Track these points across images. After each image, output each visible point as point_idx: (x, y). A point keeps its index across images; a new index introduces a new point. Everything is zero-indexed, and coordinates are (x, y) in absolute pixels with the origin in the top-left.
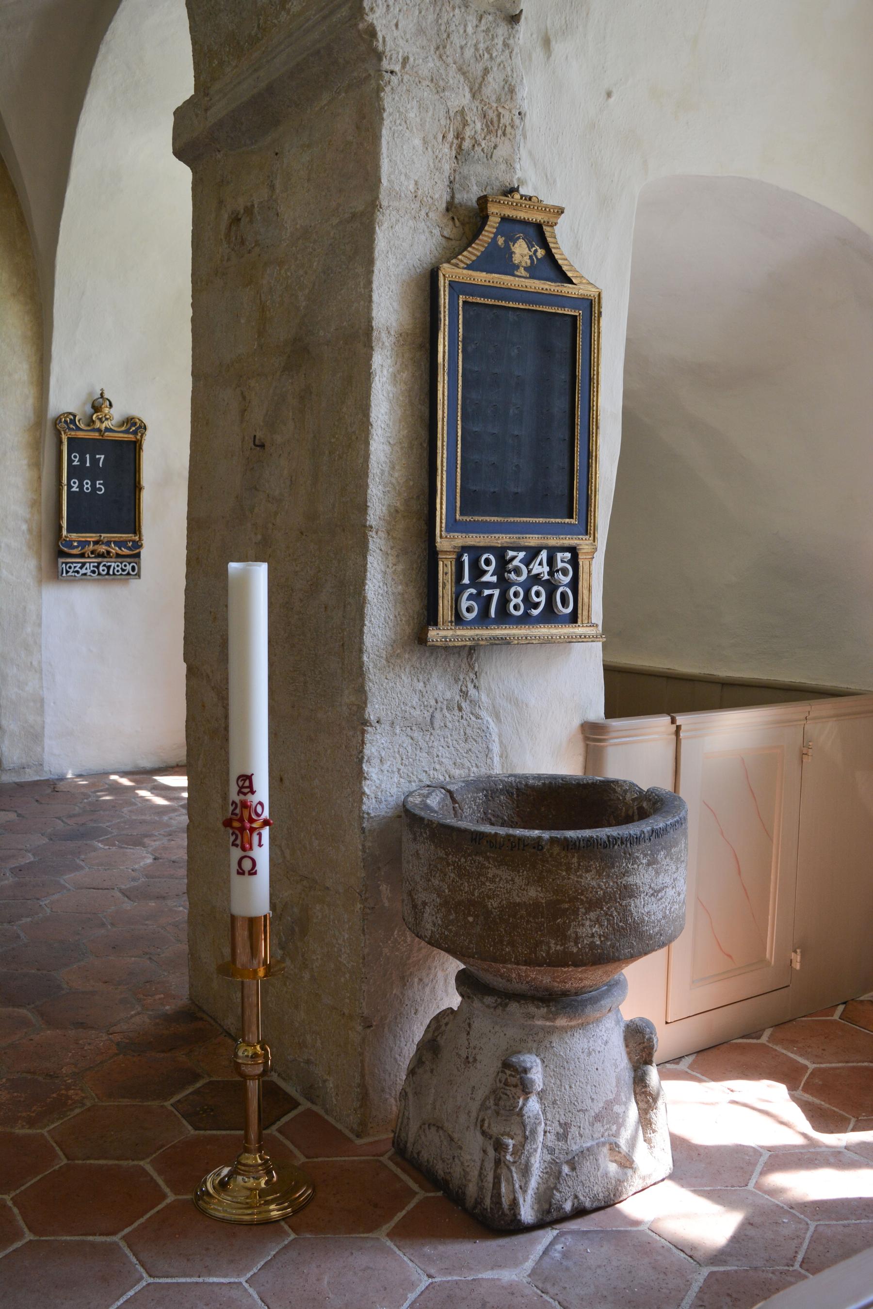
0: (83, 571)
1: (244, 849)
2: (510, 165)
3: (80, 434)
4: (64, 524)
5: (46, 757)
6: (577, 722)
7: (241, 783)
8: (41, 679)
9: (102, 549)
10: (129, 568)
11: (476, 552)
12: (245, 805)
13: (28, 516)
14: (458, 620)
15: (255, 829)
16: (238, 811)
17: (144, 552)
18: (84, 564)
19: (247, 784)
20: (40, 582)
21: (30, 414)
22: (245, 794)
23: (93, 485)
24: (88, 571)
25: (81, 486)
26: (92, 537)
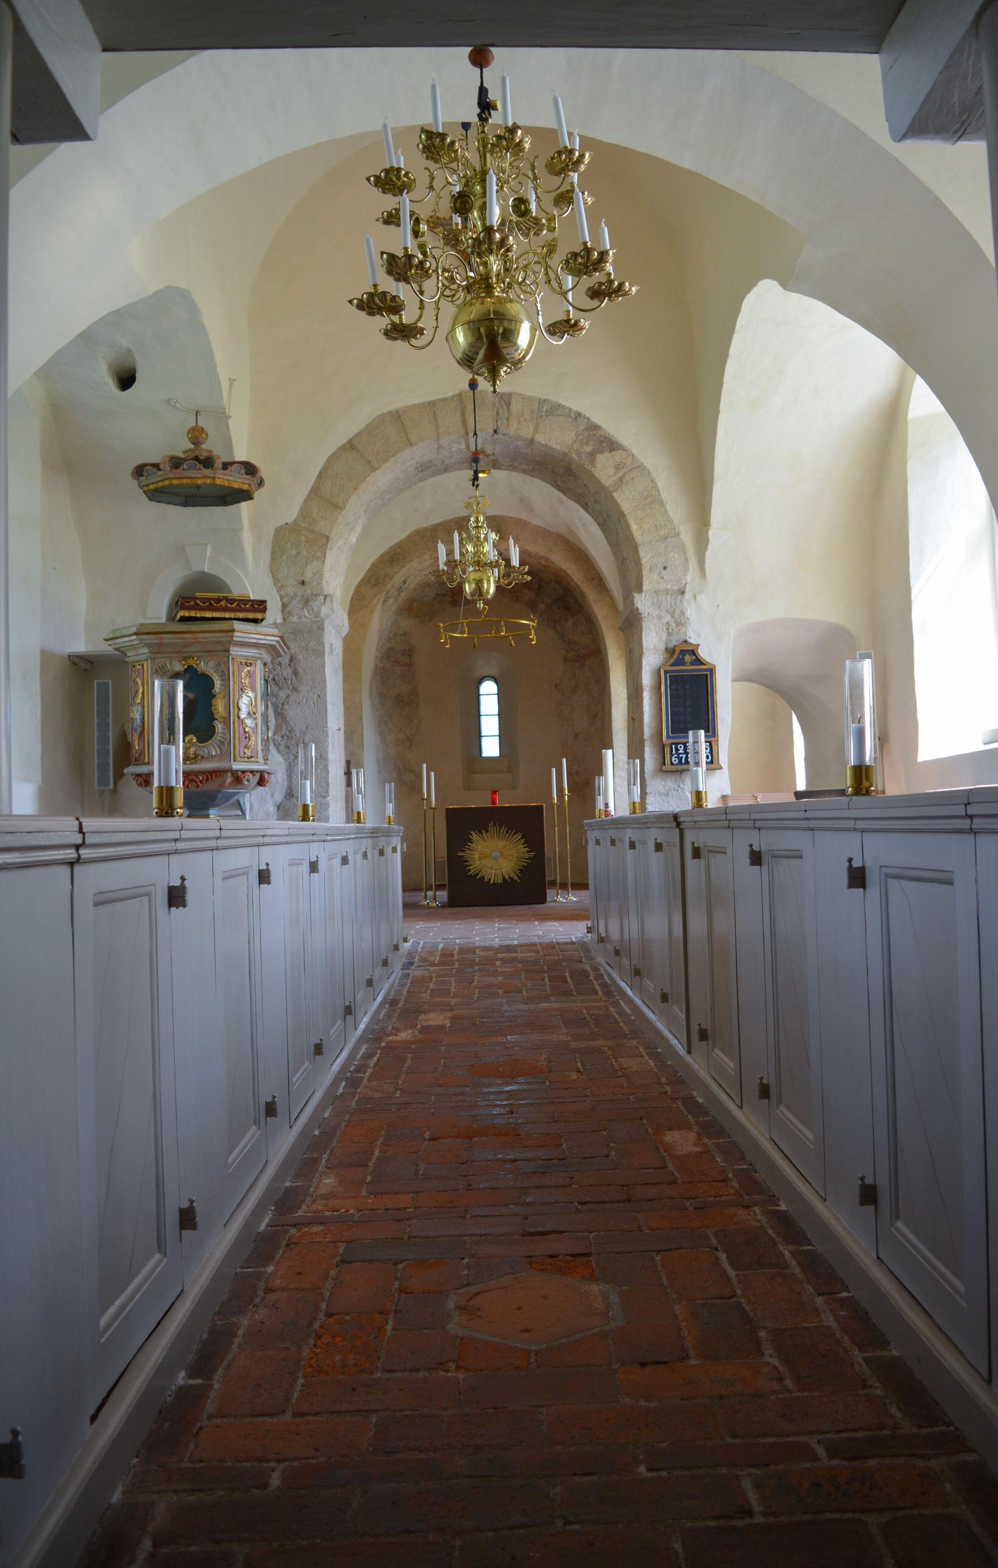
2: (685, 634)
6: (719, 795)
11: (677, 744)
14: (672, 764)
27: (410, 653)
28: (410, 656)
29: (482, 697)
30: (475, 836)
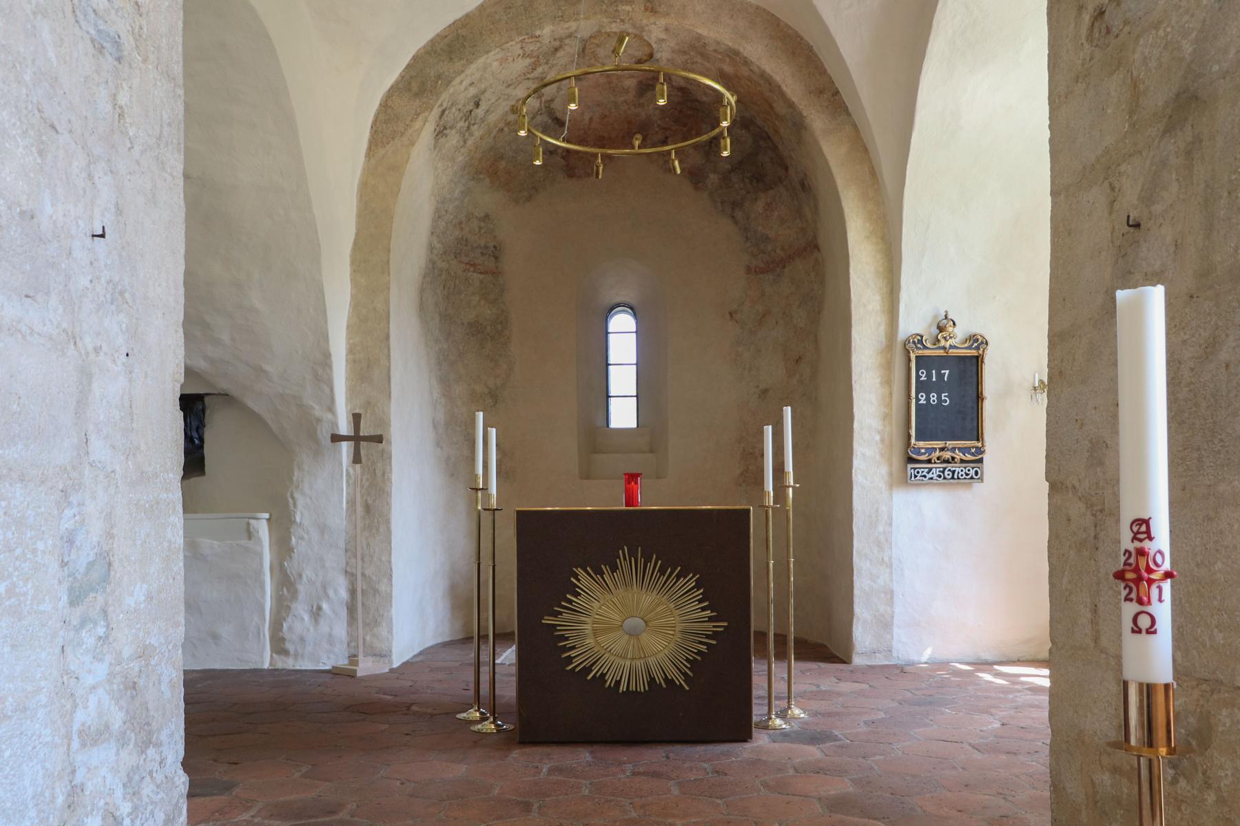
0: (930, 475)
1: (1140, 602)
3: (927, 353)
4: (913, 433)
5: (895, 645)
7: (1135, 529)
8: (891, 573)
9: (947, 455)
10: (972, 472)
12: (1141, 553)
13: (881, 428)
15: (1154, 581)
16: (1132, 560)
17: (986, 457)
18: (930, 469)
19: (1144, 528)
20: (891, 486)
21: (883, 339)
22: (1141, 540)
23: (939, 398)
24: (935, 476)
25: (928, 399)
26: (939, 444)
27: (496, 252)
28: (496, 258)
29: (611, 337)
30: (584, 579)
